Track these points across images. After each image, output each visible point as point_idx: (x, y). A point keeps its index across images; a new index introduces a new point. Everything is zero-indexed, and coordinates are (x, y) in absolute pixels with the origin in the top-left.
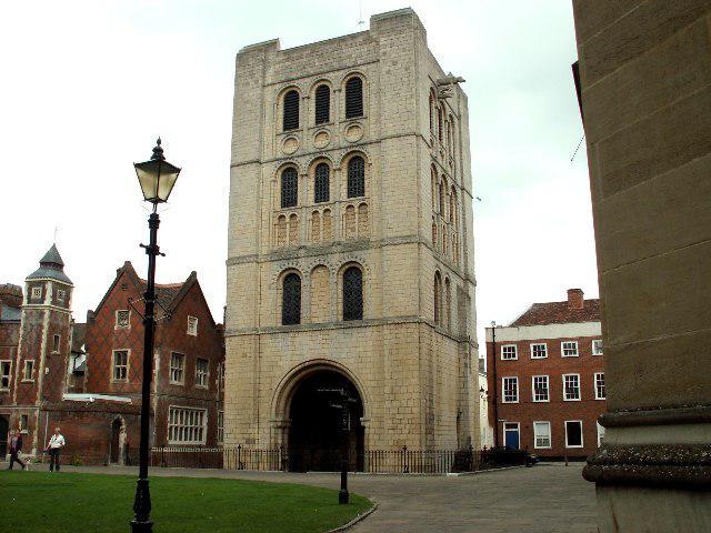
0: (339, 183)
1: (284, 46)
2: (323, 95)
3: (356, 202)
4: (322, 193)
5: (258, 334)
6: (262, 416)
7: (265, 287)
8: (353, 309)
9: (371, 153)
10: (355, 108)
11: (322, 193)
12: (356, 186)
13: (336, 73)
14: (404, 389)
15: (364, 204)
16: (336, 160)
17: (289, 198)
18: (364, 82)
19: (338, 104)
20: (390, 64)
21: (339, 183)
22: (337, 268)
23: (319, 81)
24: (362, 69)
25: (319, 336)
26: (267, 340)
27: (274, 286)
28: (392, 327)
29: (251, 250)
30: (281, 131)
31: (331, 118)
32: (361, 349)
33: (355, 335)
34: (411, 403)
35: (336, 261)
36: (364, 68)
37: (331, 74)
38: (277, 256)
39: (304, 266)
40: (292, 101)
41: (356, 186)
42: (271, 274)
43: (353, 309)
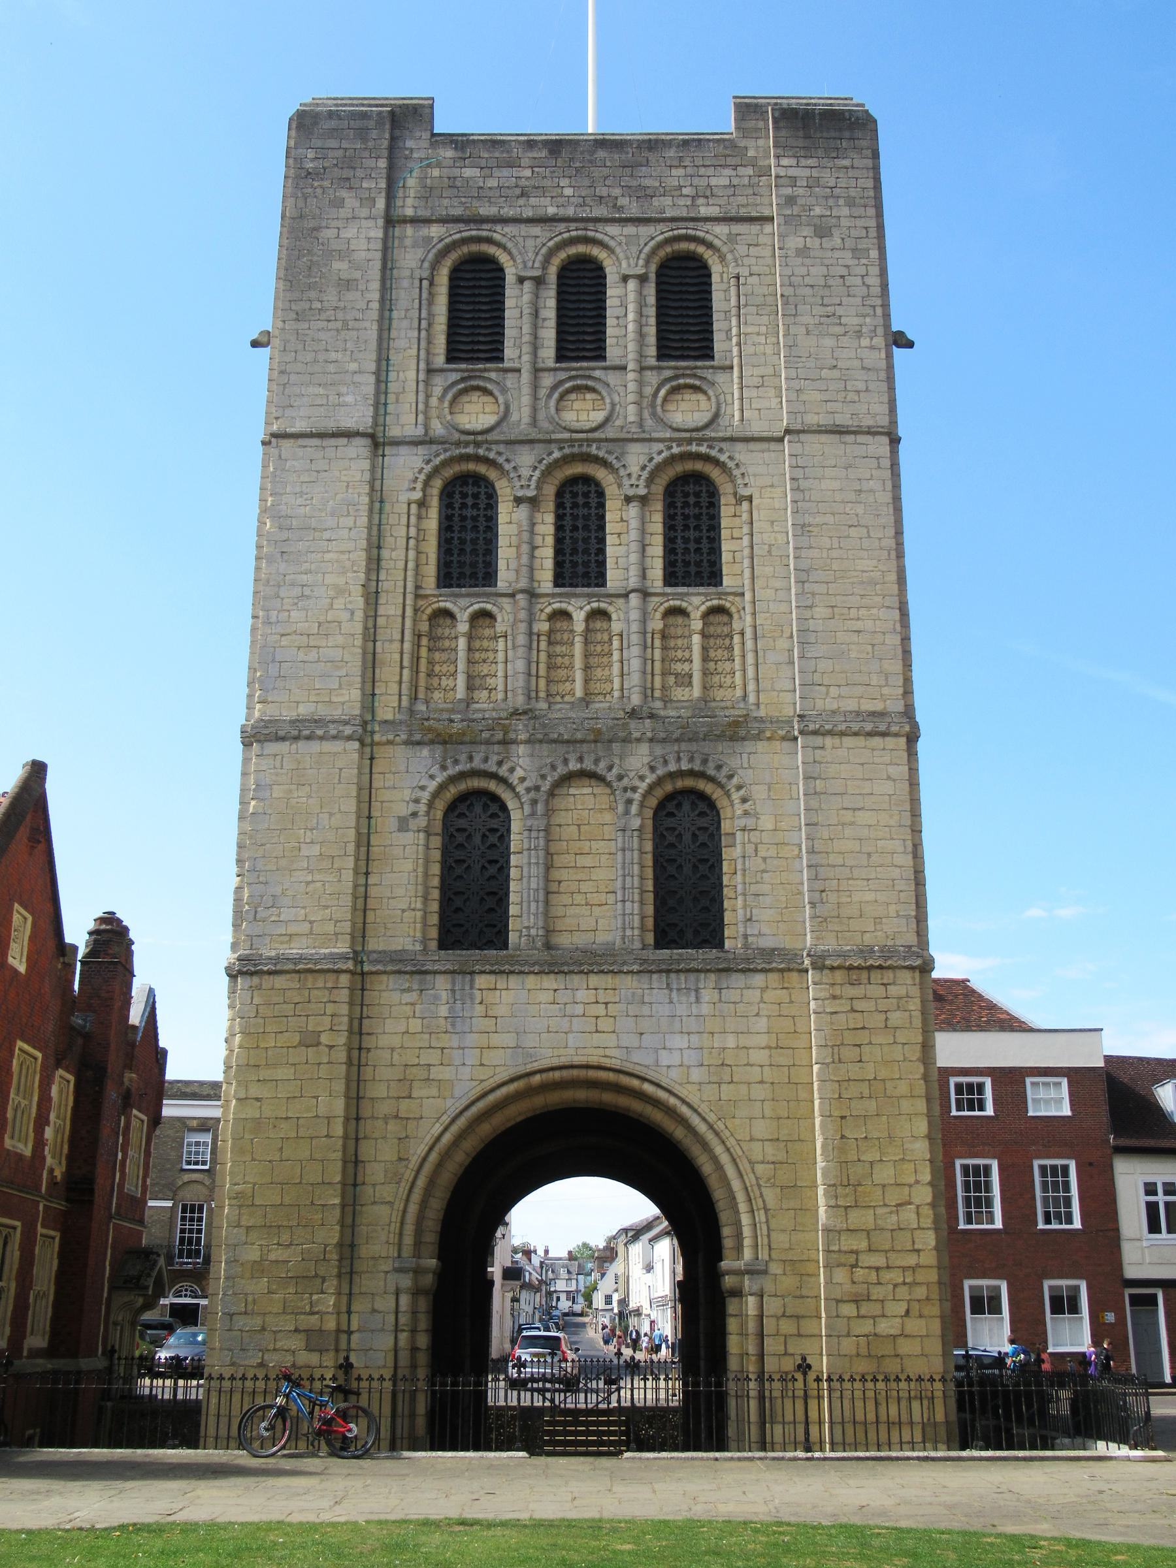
3: (697, 601)
7: (385, 823)
13: (630, 230)
14: (885, 1174)
15: (720, 610)
16: (634, 469)
18: (716, 269)
20: (808, 231)
22: (643, 786)
23: (573, 241)
27: (422, 822)
28: (839, 976)
30: (440, 360)
31: (613, 352)
32: (731, 1042)
33: (708, 995)
34: (908, 1215)
36: (721, 230)
37: (613, 229)
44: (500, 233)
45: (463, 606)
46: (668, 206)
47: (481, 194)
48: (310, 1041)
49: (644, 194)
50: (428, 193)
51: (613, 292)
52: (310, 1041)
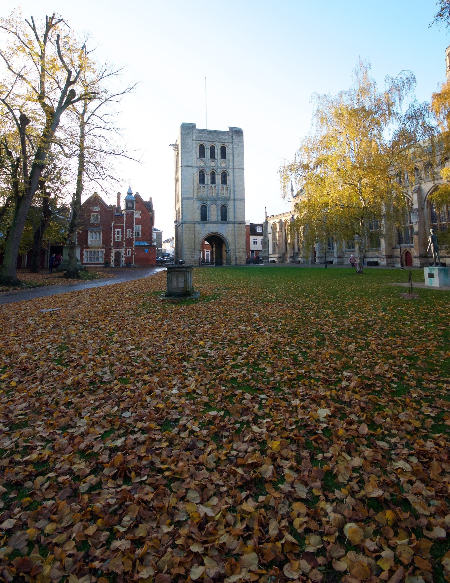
0: (219, 179)
1: (198, 127)
2: (213, 149)
3: (225, 186)
4: (213, 181)
5: (194, 223)
6: (196, 249)
8: (224, 217)
9: (230, 172)
10: (224, 156)
11: (213, 181)
12: (224, 182)
17: (202, 180)
19: (218, 153)
21: (219, 179)
24: (227, 144)
25: (215, 225)
26: (197, 225)
29: (192, 196)
31: (216, 157)
35: (220, 203)
38: (200, 199)
39: (208, 203)
40: (202, 148)
41: (224, 182)
42: (198, 205)
43: (224, 217)
44: (204, 142)
45: (202, 185)
46: (223, 141)
47: (202, 137)
48: (190, 230)
49: (220, 139)
50: (196, 137)
51: (216, 150)
52: (190, 230)
